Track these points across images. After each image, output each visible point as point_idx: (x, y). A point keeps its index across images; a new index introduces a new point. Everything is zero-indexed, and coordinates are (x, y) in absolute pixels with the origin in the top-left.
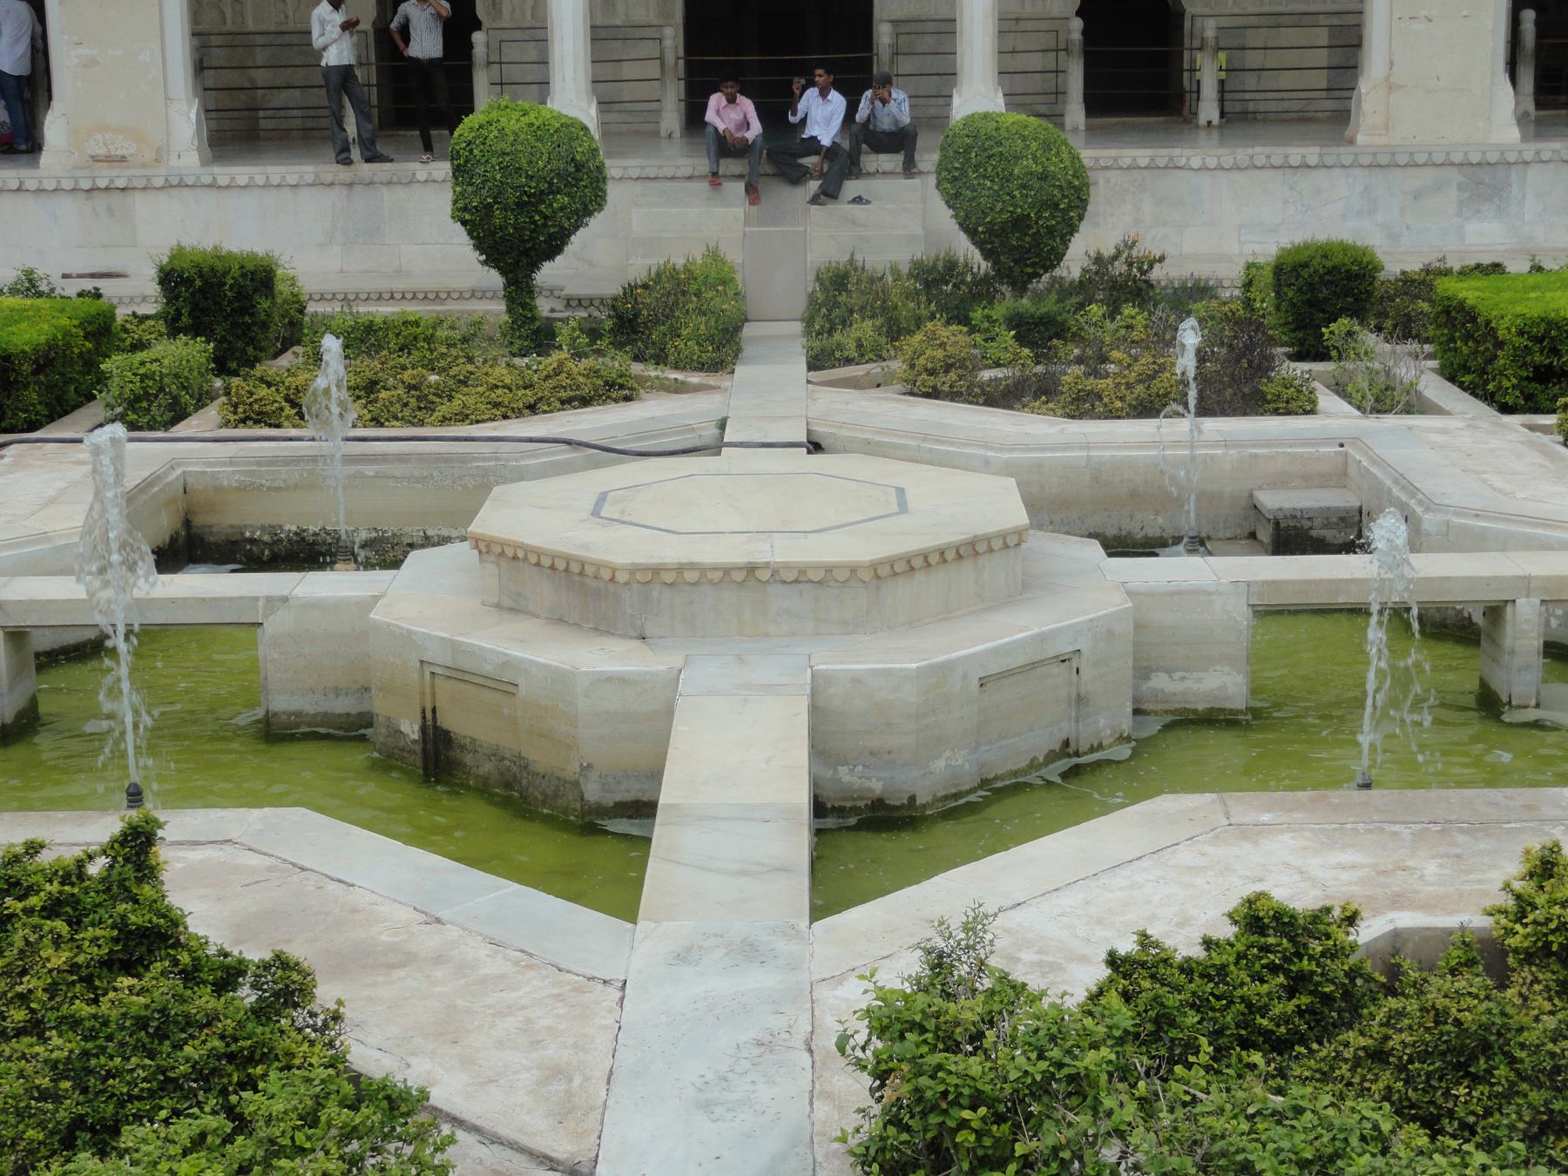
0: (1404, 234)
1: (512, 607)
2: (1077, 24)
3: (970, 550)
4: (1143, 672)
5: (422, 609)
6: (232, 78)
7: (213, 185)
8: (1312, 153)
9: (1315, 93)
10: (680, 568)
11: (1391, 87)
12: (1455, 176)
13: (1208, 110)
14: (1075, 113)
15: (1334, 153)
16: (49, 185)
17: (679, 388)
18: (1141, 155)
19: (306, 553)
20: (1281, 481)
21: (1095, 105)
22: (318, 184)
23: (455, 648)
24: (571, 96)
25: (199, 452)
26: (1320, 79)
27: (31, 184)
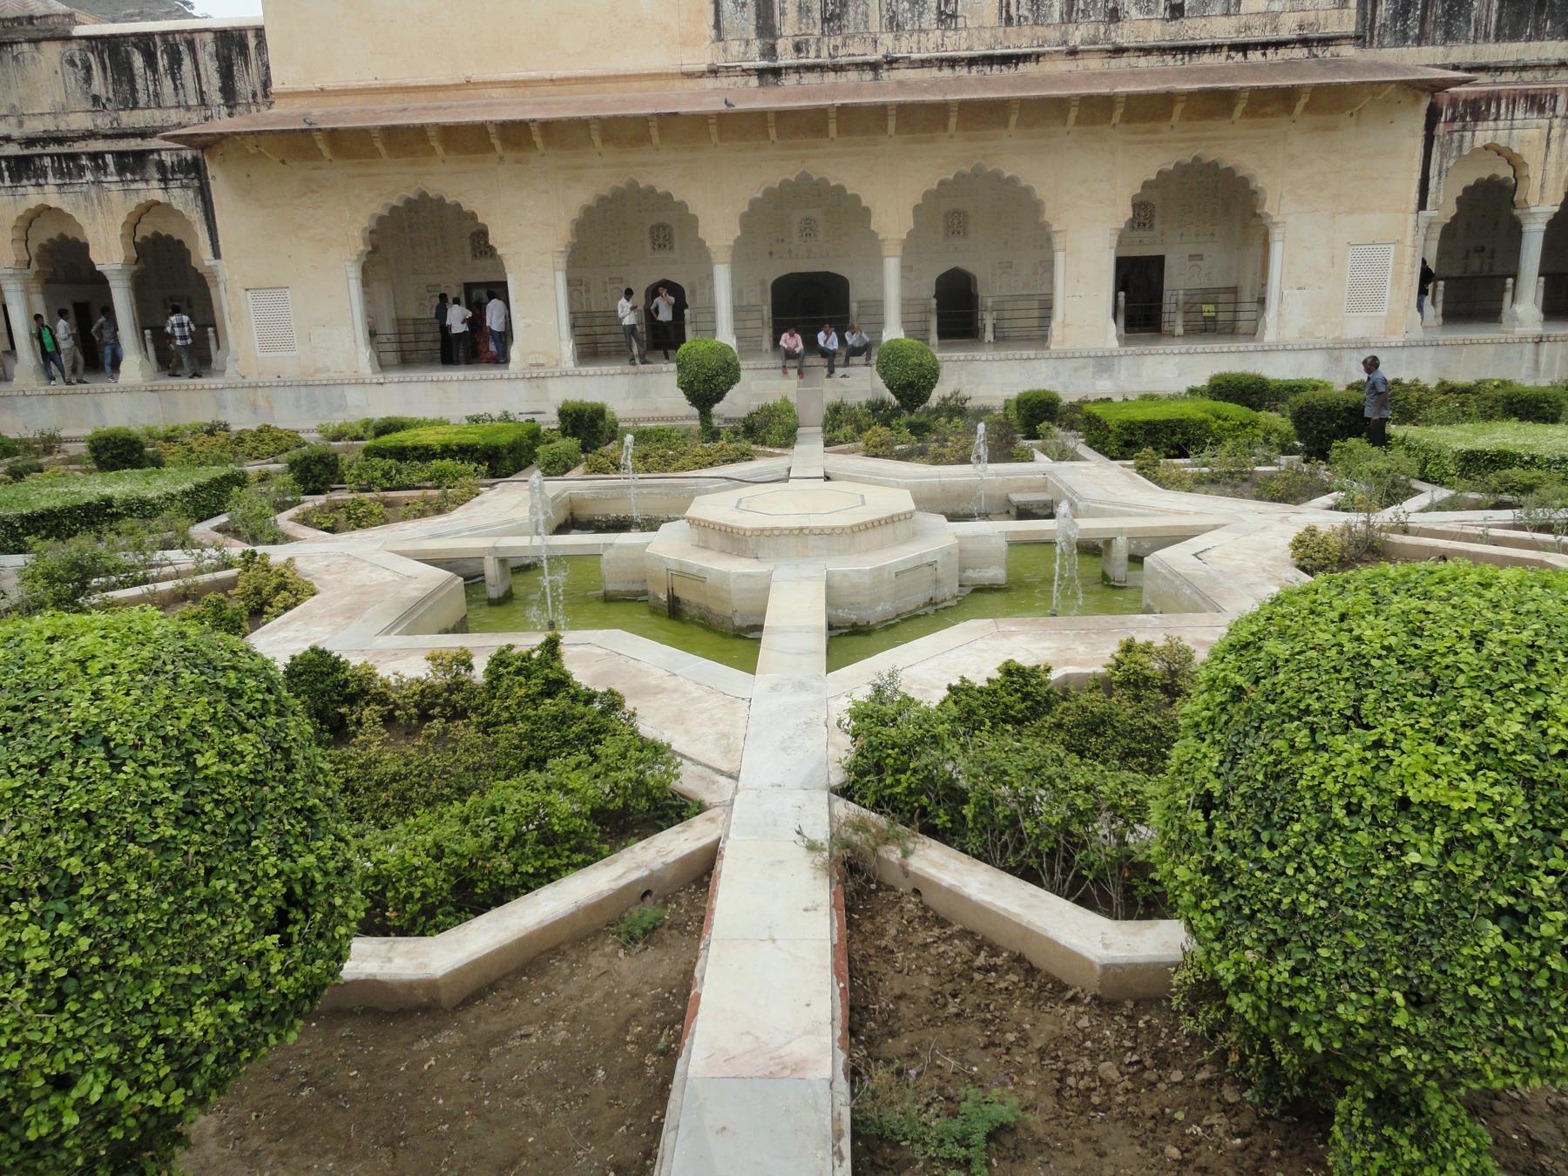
0: (1070, 386)
1: (704, 546)
2: (934, 301)
3: (891, 520)
4: (963, 569)
5: (667, 546)
6: (587, 331)
8: (1032, 353)
9: (1032, 327)
10: (772, 529)
11: (1065, 325)
12: (1091, 362)
13: (989, 336)
14: (934, 338)
15: (1041, 353)
17: (771, 455)
18: (961, 355)
19: (621, 525)
20: (1020, 490)
21: (942, 335)
22: (622, 373)
23: (681, 563)
24: (726, 335)
25: (577, 485)
26: (1035, 323)
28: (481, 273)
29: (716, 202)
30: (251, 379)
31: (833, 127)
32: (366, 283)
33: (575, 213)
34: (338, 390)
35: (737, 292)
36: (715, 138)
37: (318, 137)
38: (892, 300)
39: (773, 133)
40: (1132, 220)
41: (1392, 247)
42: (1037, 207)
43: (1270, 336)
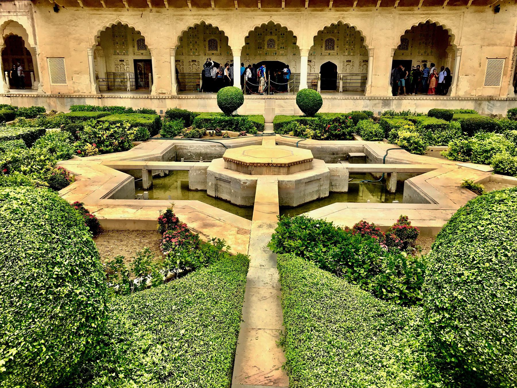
2: (320, 75)
7: (179, 98)
8: (358, 97)
12: (381, 101)
13: (341, 89)
16: (152, 97)
21: (322, 88)
27: (149, 97)
33: (180, 34)
36: (236, 6)
38: (304, 71)
39: (259, 5)
40: (400, 46)
41: (504, 60)
43: (453, 94)
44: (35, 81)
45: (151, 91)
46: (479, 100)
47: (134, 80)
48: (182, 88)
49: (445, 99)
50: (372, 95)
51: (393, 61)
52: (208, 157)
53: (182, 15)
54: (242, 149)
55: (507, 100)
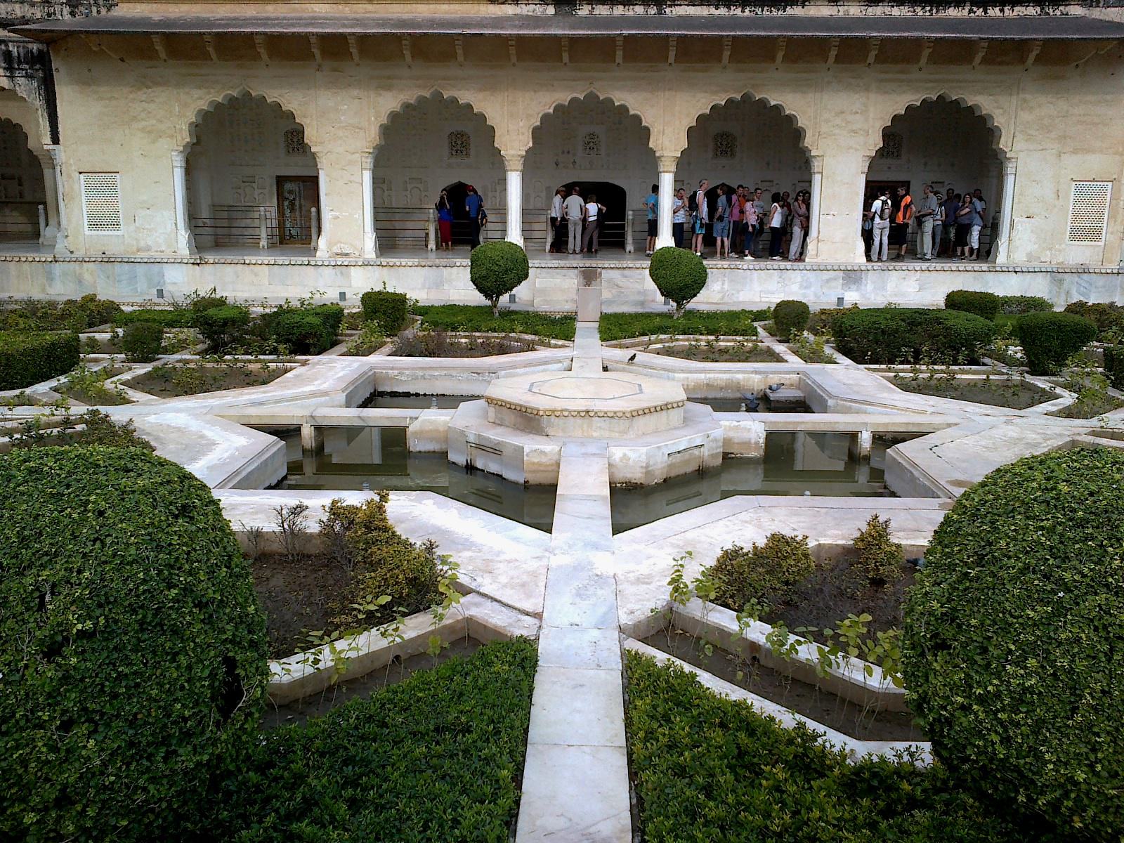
6: (388, 225)
12: (841, 273)
17: (556, 346)
24: (515, 236)
28: (294, 168)
29: (512, 118)
30: (79, 254)
31: (619, 54)
32: (189, 170)
33: (384, 120)
34: (156, 267)
35: (526, 197)
36: (514, 59)
37: (155, 39)
39: (565, 56)
41: (1110, 184)
42: (798, 134)
43: (1001, 258)
44: (47, 225)
45: (315, 250)
46: (1057, 274)
47: (275, 223)
48: (389, 241)
49: (984, 269)
50: (819, 260)
51: (867, 182)
52: (449, 401)
53: (389, 78)
54: (524, 377)
55: (1118, 273)
